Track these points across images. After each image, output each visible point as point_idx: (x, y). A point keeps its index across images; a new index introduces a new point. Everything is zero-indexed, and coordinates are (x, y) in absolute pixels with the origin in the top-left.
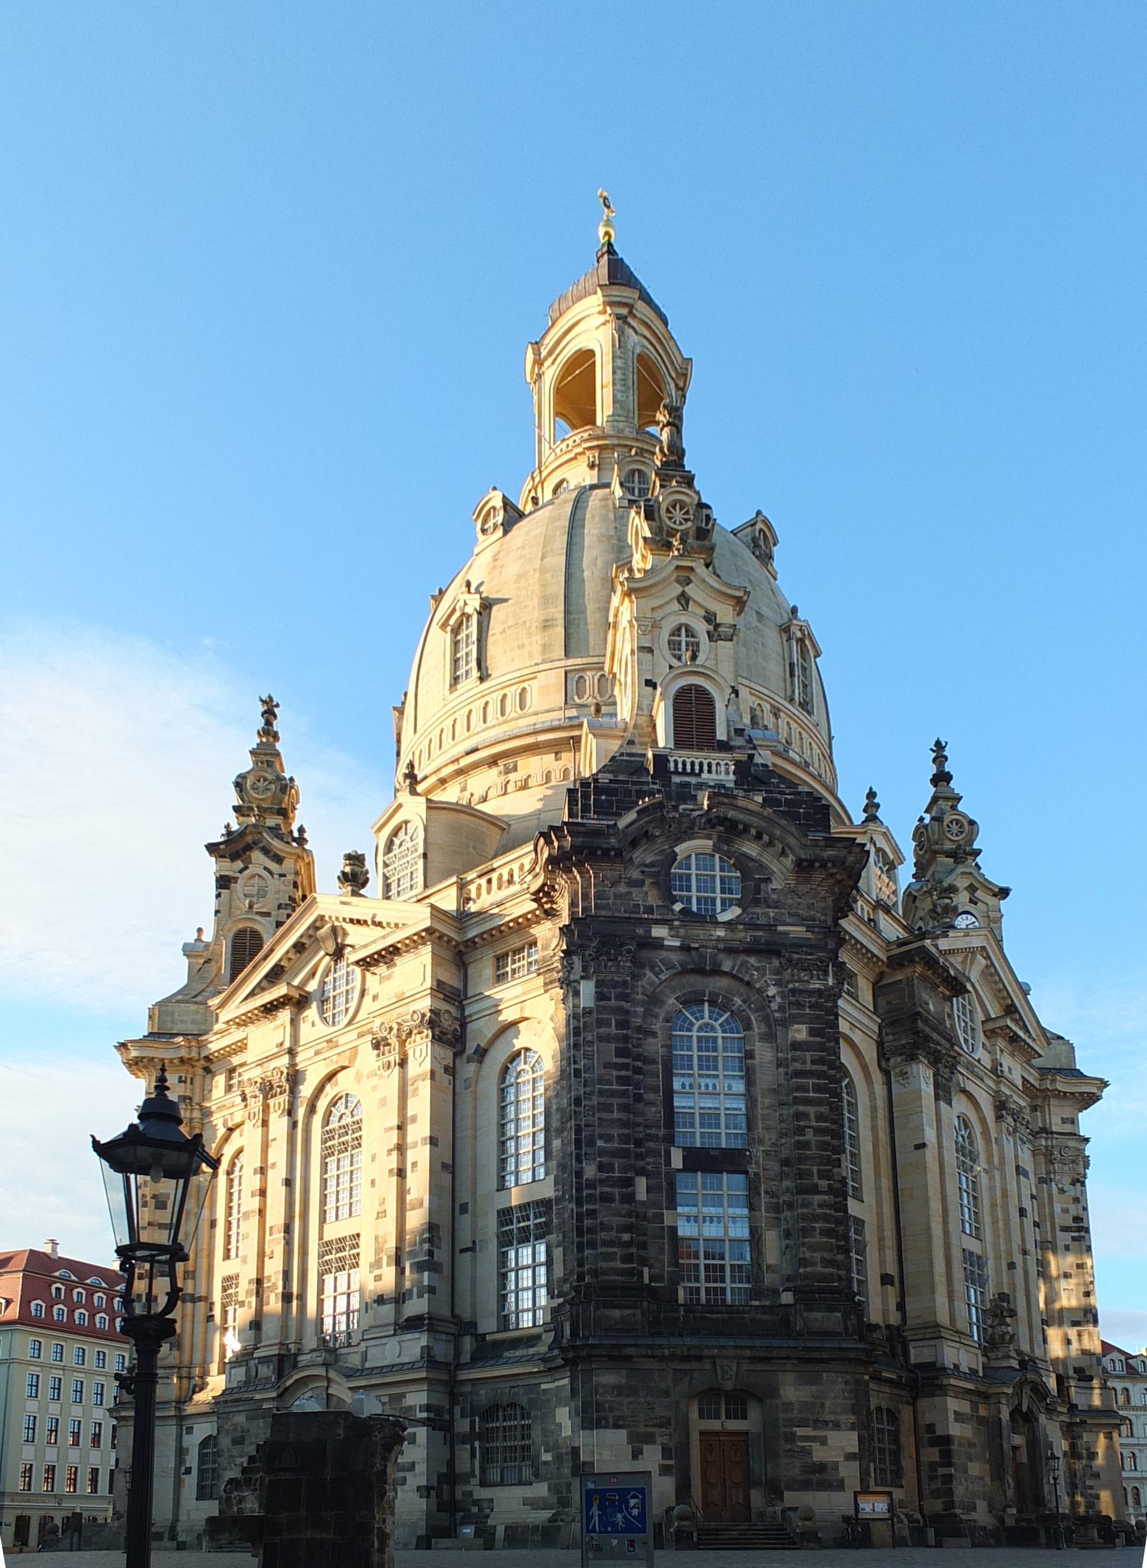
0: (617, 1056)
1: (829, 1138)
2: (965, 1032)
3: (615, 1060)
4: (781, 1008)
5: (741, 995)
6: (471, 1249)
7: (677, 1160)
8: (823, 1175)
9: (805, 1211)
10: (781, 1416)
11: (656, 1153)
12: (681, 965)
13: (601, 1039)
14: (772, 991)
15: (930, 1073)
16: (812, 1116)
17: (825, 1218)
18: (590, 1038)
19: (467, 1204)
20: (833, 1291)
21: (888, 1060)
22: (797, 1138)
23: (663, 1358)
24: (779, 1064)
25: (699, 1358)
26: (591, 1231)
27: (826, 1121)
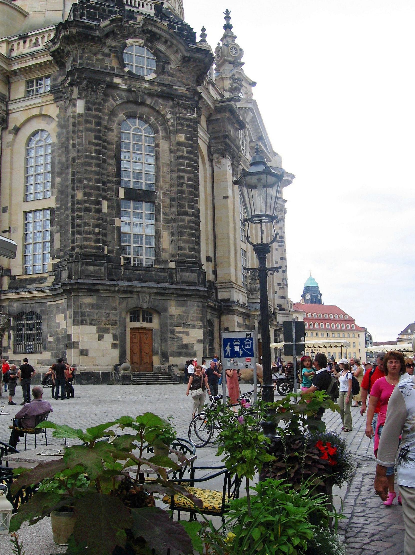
2: (243, 146)
3: (94, 141)
4: (172, 125)
5: (154, 116)
6: (9, 231)
7: (122, 194)
9: (181, 223)
10: (169, 321)
11: (112, 190)
12: (127, 98)
14: (169, 116)
15: (230, 164)
16: (186, 178)
17: (191, 228)
18: (81, 129)
19: (7, 207)
20: (193, 263)
21: (212, 155)
22: (179, 188)
23: (114, 292)
24: (171, 152)
25: (131, 292)
26: (79, 226)
27: (192, 181)
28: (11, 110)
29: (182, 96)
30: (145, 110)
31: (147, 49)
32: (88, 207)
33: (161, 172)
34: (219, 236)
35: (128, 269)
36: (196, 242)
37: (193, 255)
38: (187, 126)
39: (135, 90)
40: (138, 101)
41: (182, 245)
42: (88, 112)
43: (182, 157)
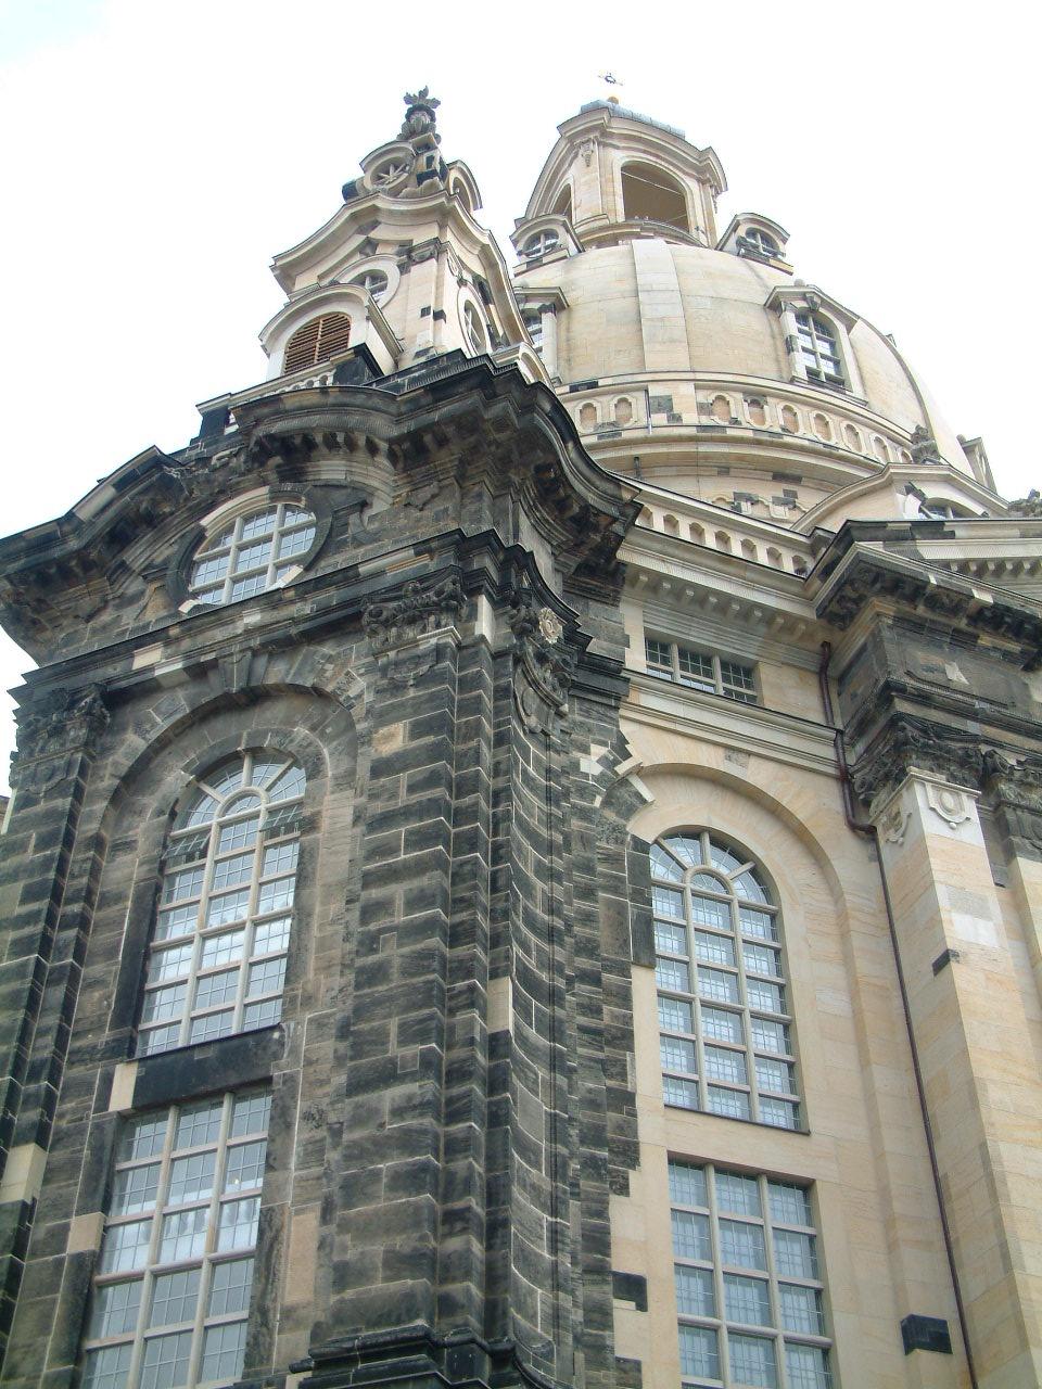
0: (24, 901)
1: (435, 942)
5: (310, 717)
8: (407, 1036)
9: (357, 1134)
11: (87, 1086)
14: (360, 684)
16: (400, 903)
21: (867, 803)
24: (357, 820)
30: (275, 712)
31: (287, 508)
33: (315, 932)
34: (954, 1186)
37: (409, 1296)
38: (420, 681)
39: (212, 656)
41: (350, 1255)
42: (24, 813)
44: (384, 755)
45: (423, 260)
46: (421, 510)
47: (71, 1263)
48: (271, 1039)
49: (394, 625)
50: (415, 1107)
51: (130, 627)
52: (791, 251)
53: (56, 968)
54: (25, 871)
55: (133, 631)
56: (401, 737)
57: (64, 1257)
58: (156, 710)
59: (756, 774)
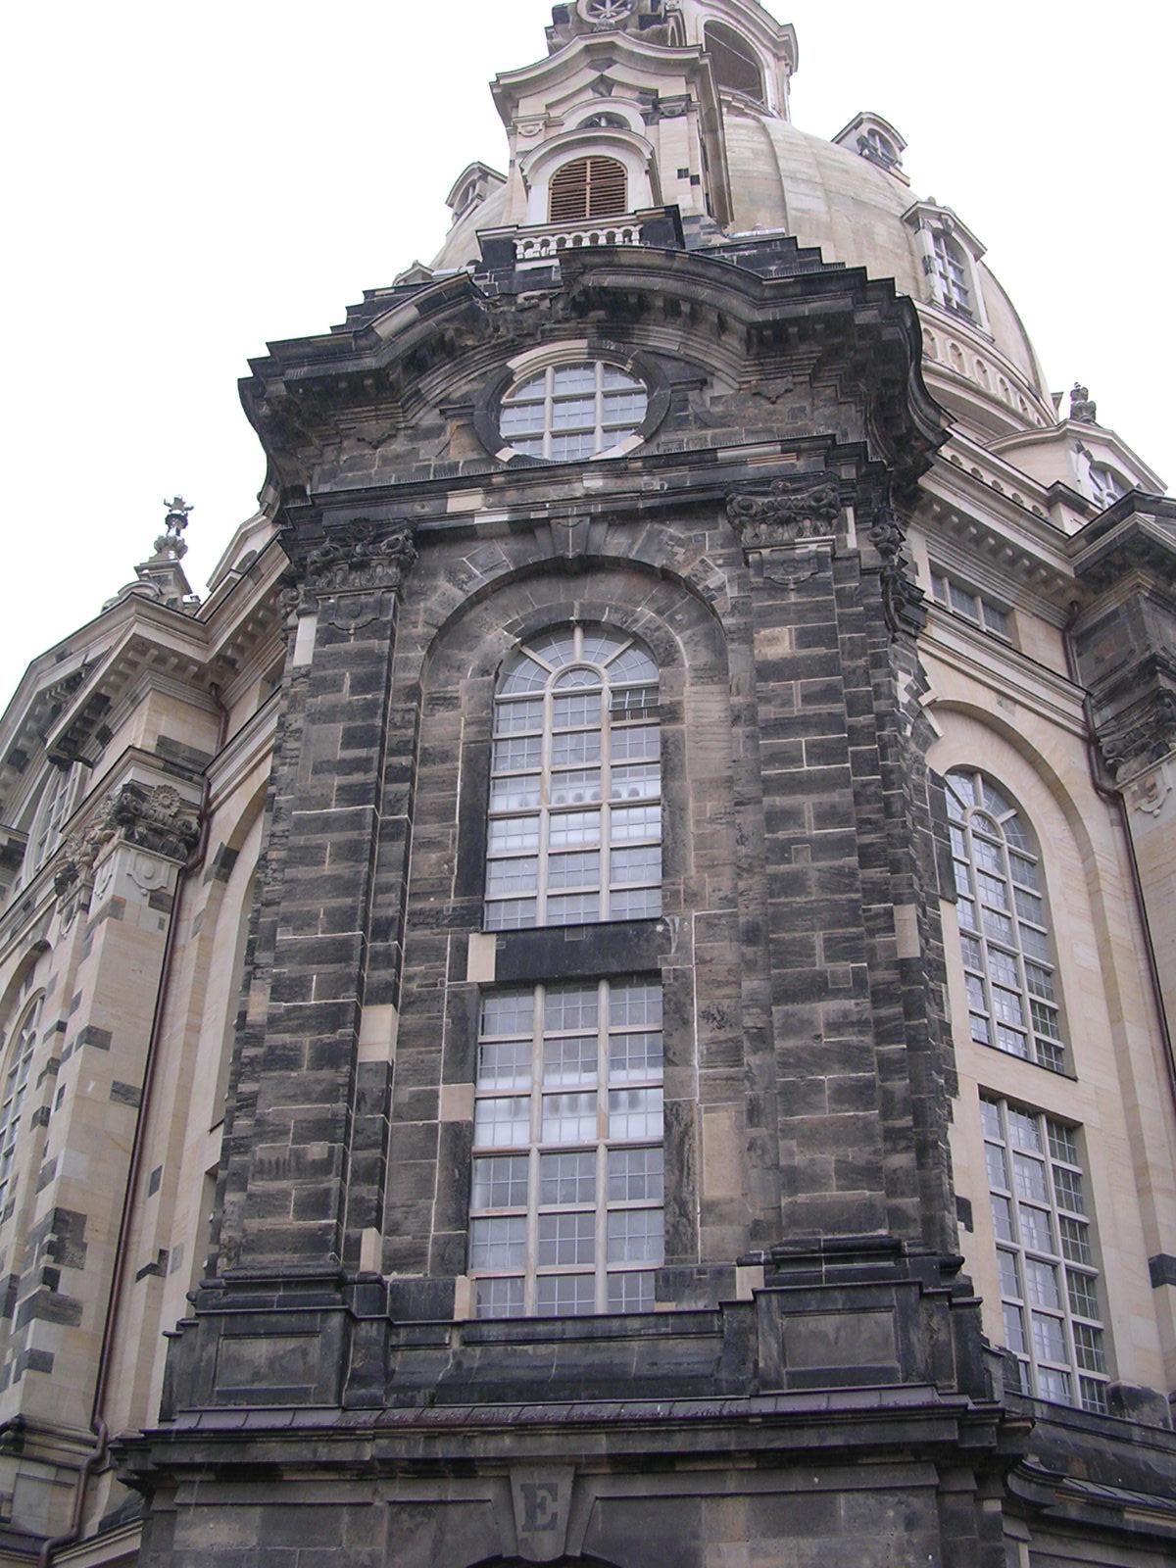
0: (346, 745)
3: (341, 754)
5: (652, 599)
7: (482, 962)
8: (837, 950)
9: (791, 1043)
11: (435, 952)
12: (515, 561)
13: (314, 718)
14: (718, 577)
16: (809, 815)
17: (850, 1057)
21: (1112, 771)
22: (771, 869)
23: (362, 1472)
25: (464, 1468)
28: (217, 796)
29: (763, 483)
31: (606, 366)
32: (284, 1047)
33: (691, 827)
35: (481, 1343)
36: (891, 1135)
37: (870, 1206)
38: (801, 587)
39: (544, 514)
40: (563, 559)
41: (798, 1160)
42: (327, 648)
43: (782, 726)
44: (770, 658)
45: (672, 115)
46: (773, 403)
47: (445, 1130)
48: (654, 931)
49: (763, 521)
50: (852, 1024)
51: (433, 463)
52: (910, 161)
53: (388, 823)
54: (343, 712)
55: (438, 469)
56: (787, 643)
57: (437, 1124)
58: (471, 559)
59: (1022, 723)
